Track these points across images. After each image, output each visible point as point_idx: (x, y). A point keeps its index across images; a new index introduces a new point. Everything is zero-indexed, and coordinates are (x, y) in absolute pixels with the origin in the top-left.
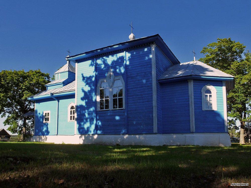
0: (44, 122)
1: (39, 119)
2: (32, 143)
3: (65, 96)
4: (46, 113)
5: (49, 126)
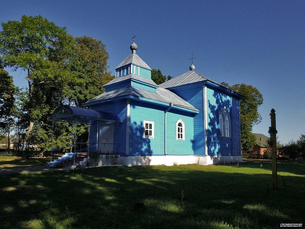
0: (144, 137)
1: (135, 131)
2: (40, 157)
3: (145, 103)
4: (148, 124)
5: (151, 144)
